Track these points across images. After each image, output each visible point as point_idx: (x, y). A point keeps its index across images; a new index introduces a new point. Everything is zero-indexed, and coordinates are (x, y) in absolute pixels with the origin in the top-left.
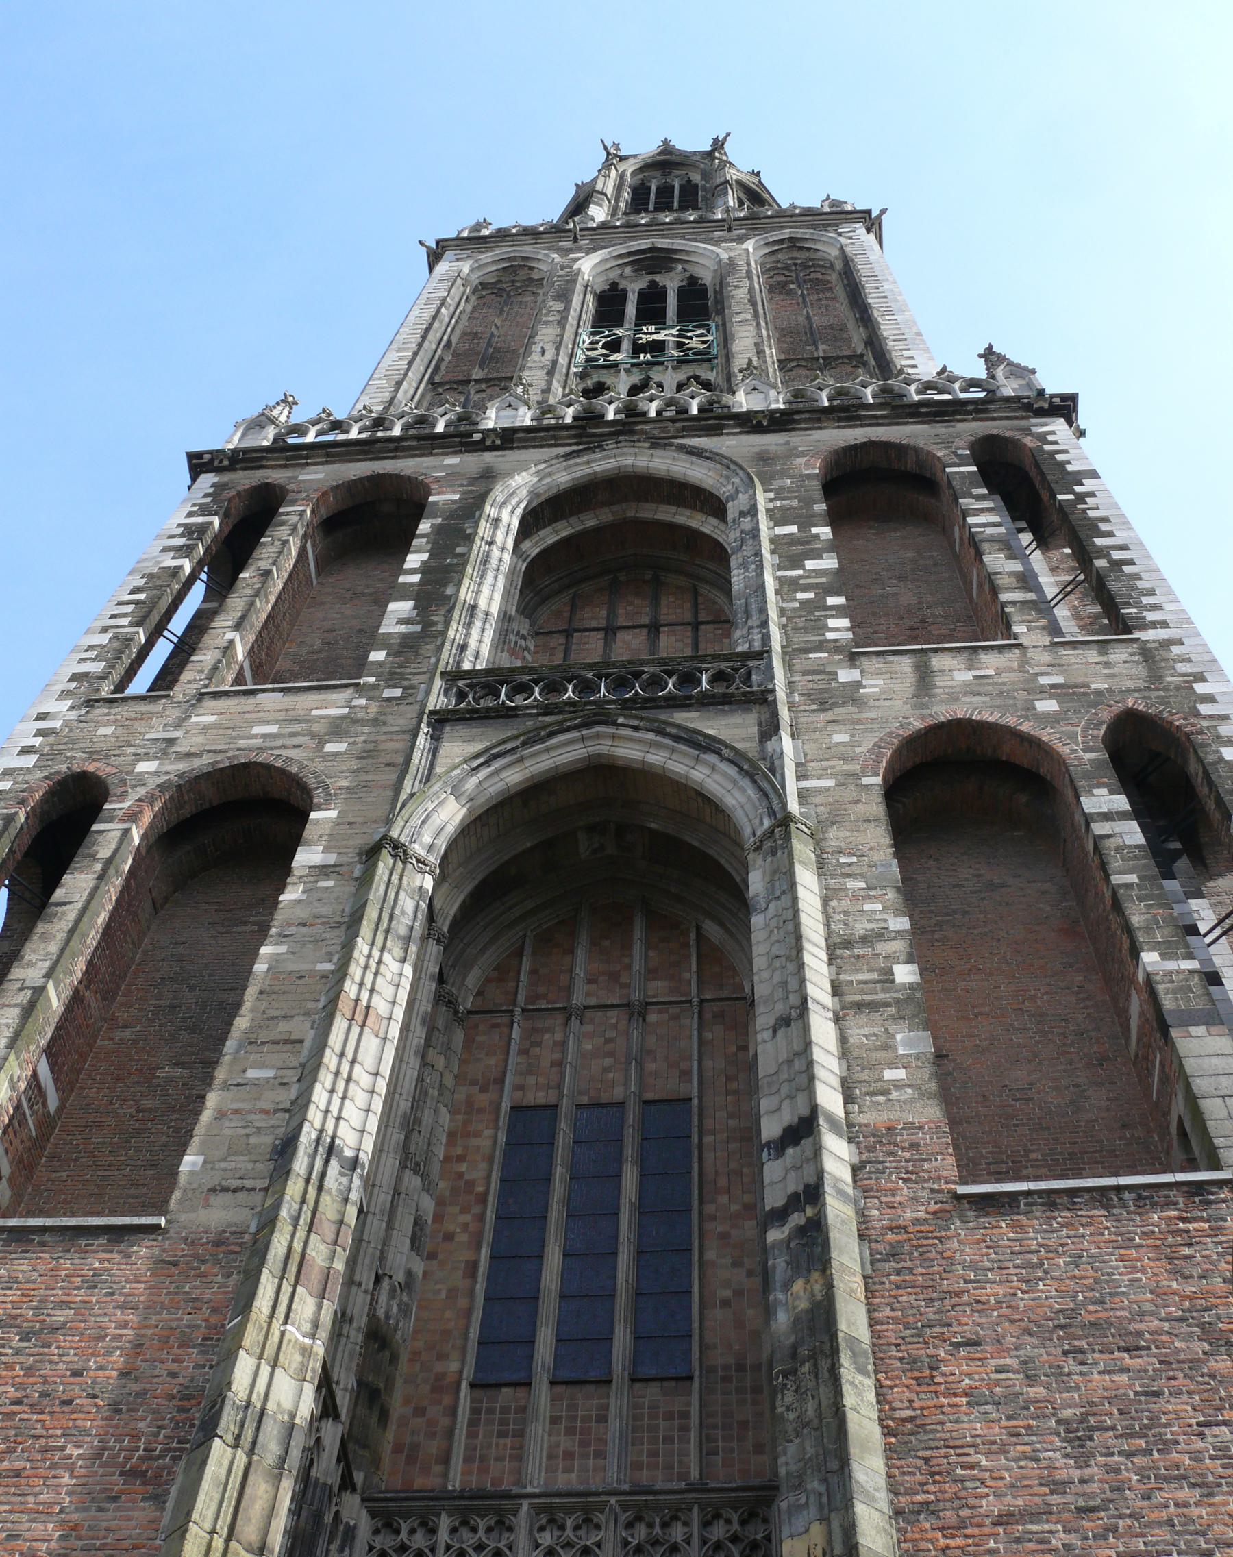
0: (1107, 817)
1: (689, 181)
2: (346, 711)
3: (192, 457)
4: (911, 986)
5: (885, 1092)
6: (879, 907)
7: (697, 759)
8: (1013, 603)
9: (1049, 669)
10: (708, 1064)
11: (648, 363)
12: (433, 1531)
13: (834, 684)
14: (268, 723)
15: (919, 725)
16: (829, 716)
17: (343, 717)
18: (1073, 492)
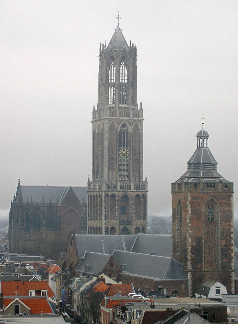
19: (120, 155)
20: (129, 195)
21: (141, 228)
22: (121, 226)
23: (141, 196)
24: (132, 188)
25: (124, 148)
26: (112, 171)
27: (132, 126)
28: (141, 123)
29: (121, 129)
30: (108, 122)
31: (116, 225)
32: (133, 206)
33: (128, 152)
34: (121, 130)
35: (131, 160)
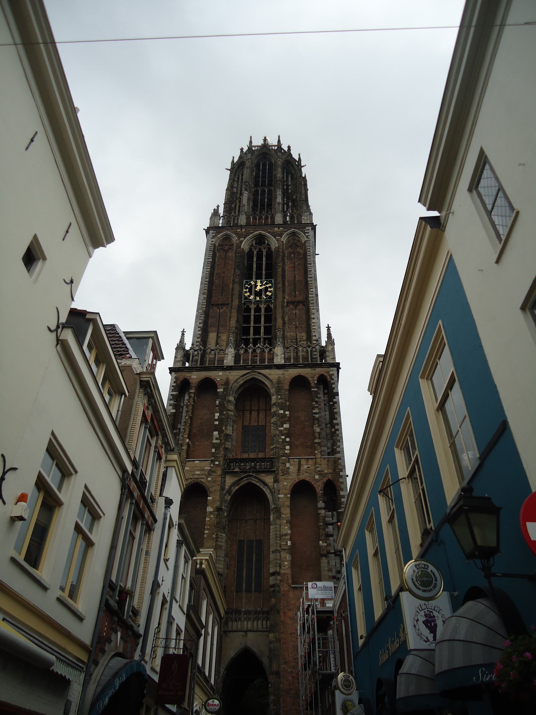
0: (321, 509)
1: (271, 162)
2: (210, 468)
3: (169, 368)
4: (289, 546)
5: (285, 567)
6: (287, 527)
7: (264, 487)
8: (316, 443)
9: (318, 466)
10: (265, 533)
11: (258, 301)
12: (232, 615)
13: (286, 468)
14: (198, 470)
15: (297, 481)
16: (284, 477)
17: (210, 470)
18: (333, 401)
19: (248, 294)
20: (267, 377)
21: (319, 488)
22: (229, 480)
23: (313, 381)
24: (279, 360)
25: (259, 282)
26: (218, 333)
27: (281, 237)
28: (305, 231)
29: (251, 249)
30: (214, 234)
31: (209, 475)
32: (281, 412)
33: (270, 287)
34: (253, 250)
35: (279, 300)
